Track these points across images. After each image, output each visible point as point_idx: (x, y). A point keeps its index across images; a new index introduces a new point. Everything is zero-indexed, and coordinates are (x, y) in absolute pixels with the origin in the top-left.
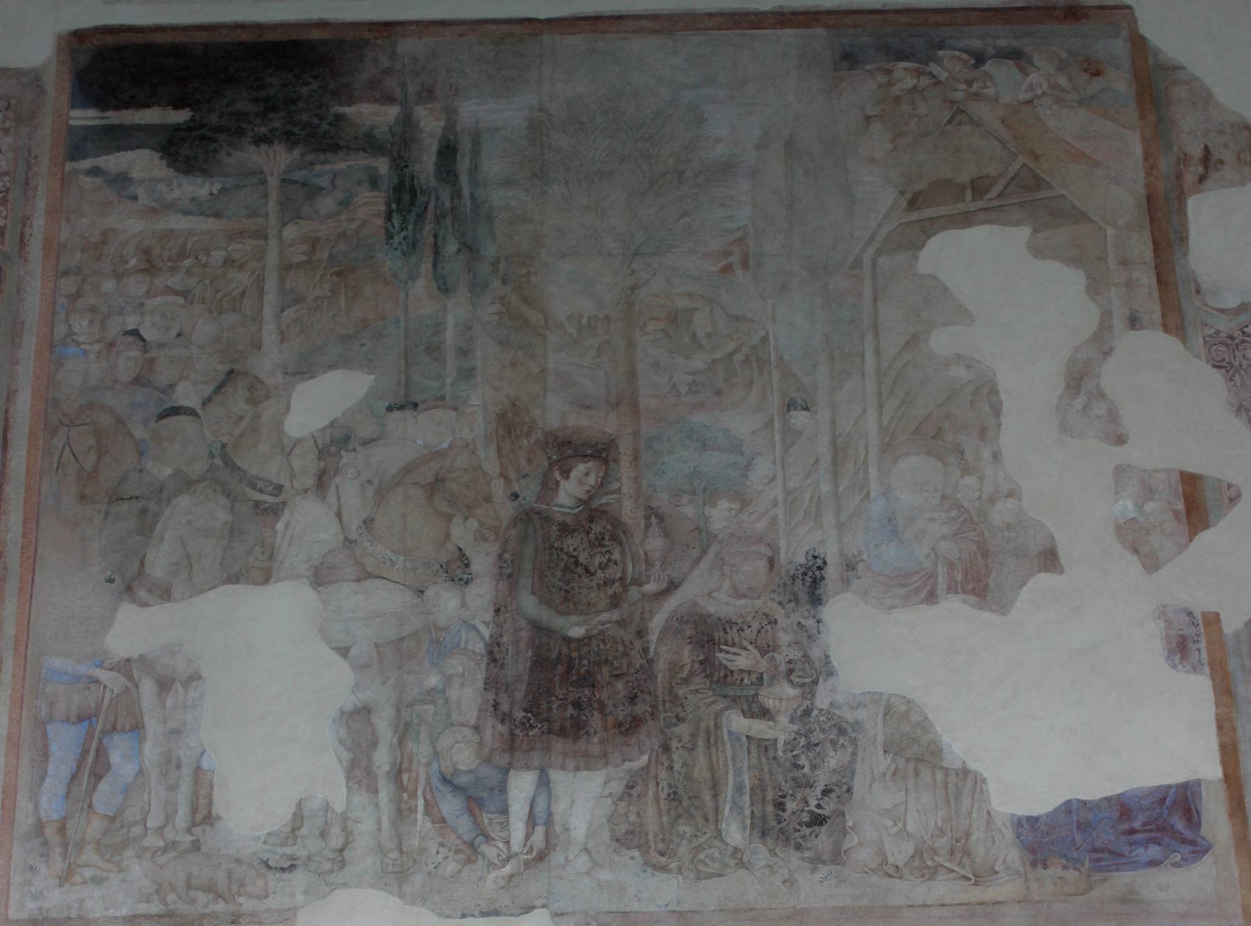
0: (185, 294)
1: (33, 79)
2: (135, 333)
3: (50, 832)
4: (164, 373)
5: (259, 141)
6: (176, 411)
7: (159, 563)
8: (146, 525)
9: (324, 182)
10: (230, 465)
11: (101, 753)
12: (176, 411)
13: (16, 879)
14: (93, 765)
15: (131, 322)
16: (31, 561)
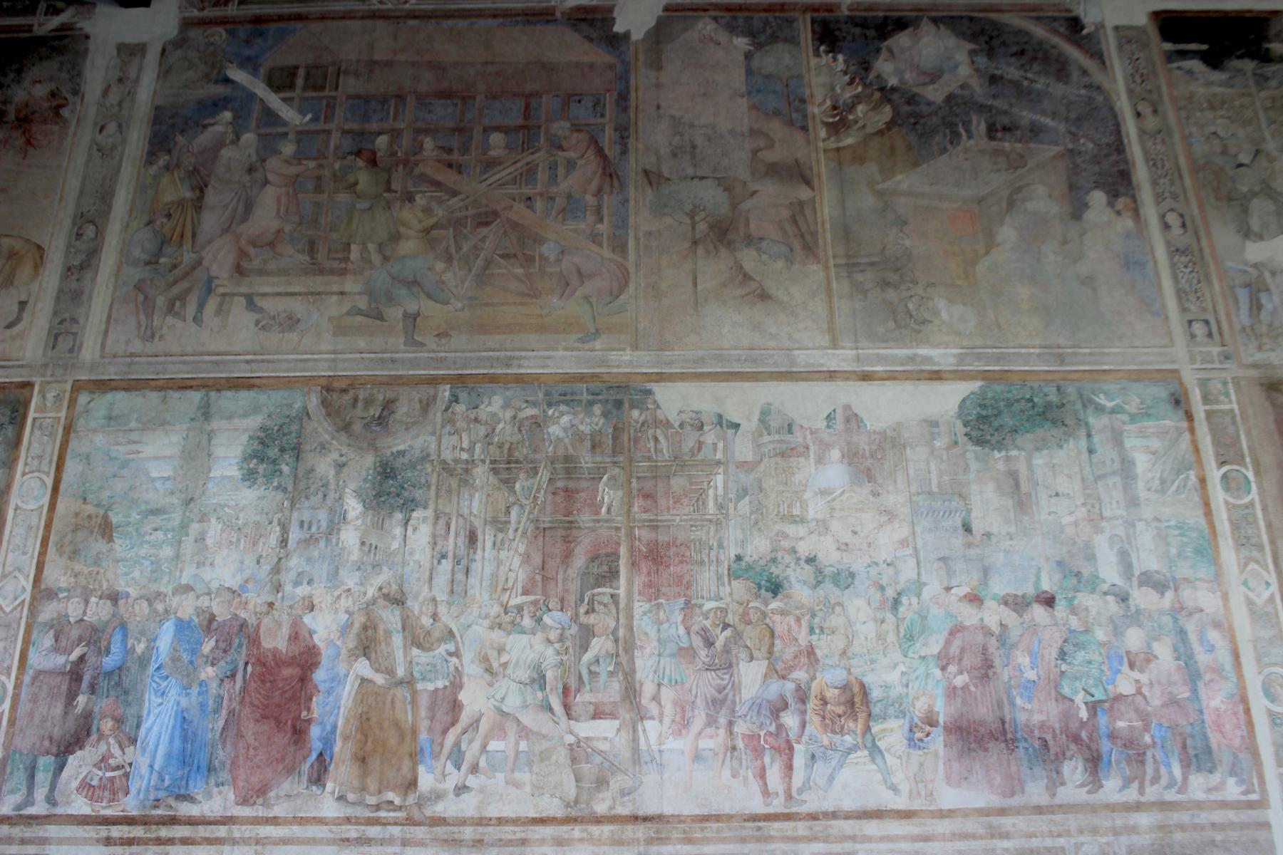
0: (1229, 118)
1: (1142, 30)
2: (1214, 133)
3: (1248, 330)
4: (1233, 150)
5: (1239, 57)
6: (1240, 165)
7: (1255, 224)
8: (1245, 211)
9: (1269, 74)
10: (1269, 187)
11: (1258, 300)
12: (1240, 165)
13: (1242, 348)
14: (1256, 306)
15: (1212, 129)
16: (1206, 224)
